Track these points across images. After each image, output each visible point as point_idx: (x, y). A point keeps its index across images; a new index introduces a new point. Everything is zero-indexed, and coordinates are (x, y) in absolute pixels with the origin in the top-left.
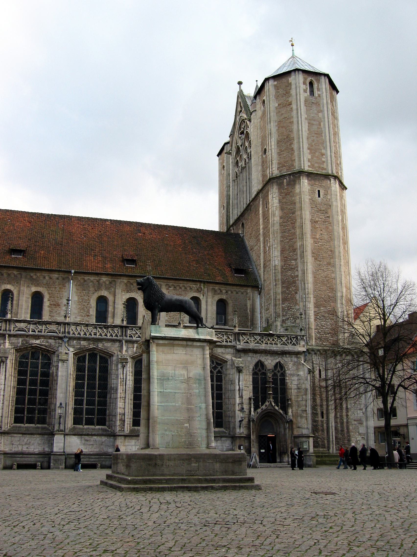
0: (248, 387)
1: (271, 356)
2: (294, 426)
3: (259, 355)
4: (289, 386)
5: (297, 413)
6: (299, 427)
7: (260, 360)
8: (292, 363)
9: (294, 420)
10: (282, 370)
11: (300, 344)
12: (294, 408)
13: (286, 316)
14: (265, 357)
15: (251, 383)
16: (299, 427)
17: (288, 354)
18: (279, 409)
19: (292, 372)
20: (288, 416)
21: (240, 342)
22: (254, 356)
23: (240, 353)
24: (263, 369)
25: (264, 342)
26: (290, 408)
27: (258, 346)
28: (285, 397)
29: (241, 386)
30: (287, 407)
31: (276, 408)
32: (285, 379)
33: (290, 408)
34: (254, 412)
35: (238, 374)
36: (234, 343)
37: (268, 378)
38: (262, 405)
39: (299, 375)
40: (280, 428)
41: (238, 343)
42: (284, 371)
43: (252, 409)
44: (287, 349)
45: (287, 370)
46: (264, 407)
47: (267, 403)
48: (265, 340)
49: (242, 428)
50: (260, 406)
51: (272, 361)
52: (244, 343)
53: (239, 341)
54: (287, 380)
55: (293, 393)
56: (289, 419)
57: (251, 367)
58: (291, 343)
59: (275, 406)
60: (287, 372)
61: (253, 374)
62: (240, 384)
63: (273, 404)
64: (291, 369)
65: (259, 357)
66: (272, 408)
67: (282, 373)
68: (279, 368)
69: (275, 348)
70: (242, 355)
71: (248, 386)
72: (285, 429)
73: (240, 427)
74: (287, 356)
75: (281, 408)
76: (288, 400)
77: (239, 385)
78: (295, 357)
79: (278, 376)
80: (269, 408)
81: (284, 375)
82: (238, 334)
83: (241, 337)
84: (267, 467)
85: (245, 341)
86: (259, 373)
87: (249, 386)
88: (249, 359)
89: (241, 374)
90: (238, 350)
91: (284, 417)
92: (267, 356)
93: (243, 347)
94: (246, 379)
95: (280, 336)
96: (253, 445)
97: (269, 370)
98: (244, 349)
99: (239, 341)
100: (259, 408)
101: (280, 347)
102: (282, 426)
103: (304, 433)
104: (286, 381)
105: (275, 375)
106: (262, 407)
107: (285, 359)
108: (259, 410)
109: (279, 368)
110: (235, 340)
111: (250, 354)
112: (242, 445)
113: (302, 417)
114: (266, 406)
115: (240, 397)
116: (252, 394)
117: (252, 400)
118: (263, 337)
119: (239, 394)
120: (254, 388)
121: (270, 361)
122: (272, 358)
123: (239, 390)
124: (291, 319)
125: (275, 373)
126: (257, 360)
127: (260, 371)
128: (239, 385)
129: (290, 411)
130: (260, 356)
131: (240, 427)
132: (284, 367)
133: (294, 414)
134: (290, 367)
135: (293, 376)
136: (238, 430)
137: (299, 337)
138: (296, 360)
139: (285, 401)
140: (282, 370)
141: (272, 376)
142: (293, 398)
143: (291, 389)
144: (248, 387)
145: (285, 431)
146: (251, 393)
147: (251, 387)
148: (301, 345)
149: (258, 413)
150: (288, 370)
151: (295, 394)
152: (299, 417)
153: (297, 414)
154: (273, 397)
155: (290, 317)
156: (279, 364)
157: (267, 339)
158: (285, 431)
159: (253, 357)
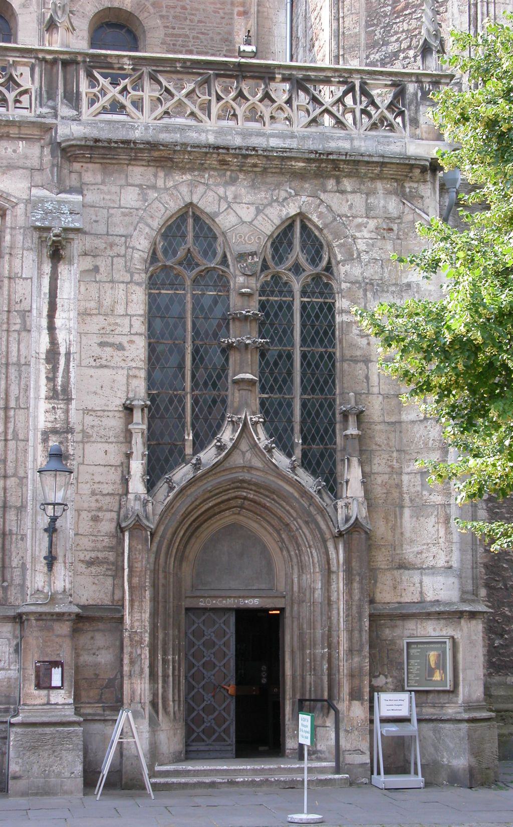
0: (120, 347)
1: (253, 186)
2: (381, 559)
3: (188, 177)
4: (353, 346)
5: (399, 486)
6: (403, 566)
7: (191, 204)
8: (372, 224)
9: (381, 529)
10: (315, 259)
11: (415, 122)
12: (379, 465)
13: (386, 43)
14: (221, 191)
15: (139, 326)
16: (403, 566)
17: (349, 175)
18: (293, 469)
19: (371, 272)
20: (341, 503)
21: (77, 107)
22: (160, 183)
23: (77, 166)
24: (209, 251)
25: (215, 108)
26: (355, 461)
27: (182, 129)
28: (331, 406)
29: (61, 336)
30: (338, 456)
31: (280, 459)
32: (331, 308)
33: (355, 461)
34: (150, 485)
35: (47, 268)
36: (45, 110)
37: (235, 301)
38: (199, 445)
39: (409, 285)
40: (302, 568)
41: (65, 111)
42: (328, 268)
43: (137, 466)
44: (346, 145)
45: (344, 262)
46: (209, 456)
47: (227, 435)
48: (219, 98)
49: (59, 567)
50: (189, 450)
51: (258, 211)
52: (105, 110)
53: (73, 99)
54: (342, 311)
55: (374, 379)
56: (347, 519)
57: (142, 244)
58: (364, 112)
59: (270, 450)
60: (343, 269)
61: (153, 283)
62: (58, 322)
63: (262, 439)
64: (365, 257)
65: (184, 190)
66: (257, 463)
67: (317, 278)
68: (297, 253)
69: (274, 142)
70: (91, 174)
71: (117, 340)
72: (328, 572)
73: (51, 560)
74: (348, 184)
75: (309, 463)
76: (345, 415)
77: (51, 328)
78: (388, 193)
79: (291, 293)
80: (237, 459)
81: (327, 285)
82: (65, 64)
83: (84, 86)
84: (213, 785)
85: (104, 101)
86: (189, 276)
87: (124, 340)
88: (130, 197)
89: (63, 268)
90: (64, 150)
91: (322, 511)
92: (233, 181)
93: (95, 133)
94: (107, 302)
95: (308, 79)
96: (132, 662)
97: (242, 257)
98: (97, 141)
99: (73, 99)
100: (182, 459)
101: (304, 138)
102: (314, 557)
103: (430, 596)
104: (338, 319)
105: (276, 285)
106: (201, 455)
107: (334, 200)
108: (182, 474)
109: (297, 253)
110: (51, 96)
111: (139, 173)
112: (56, 664)
113: (420, 509)
114: (220, 448)
115: (53, 395)
116: (140, 387)
117: (137, 416)
118: (207, 81)
119: (51, 379)
120: (154, 357)
121: (247, 213)
122: (262, 196)
123: (52, 355)
124: (405, 58)
125: (276, 277)
126: (173, 206)
127: (189, 261)
128: (51, 328)
129: (353, 475)
130: (192, 185)
131: (51, 560)
132: (329, 246)
133: (379, 491)
134: (361, 245)
135: (375, 294)
136: (38, 580)
137: (411, 88)
138: (393, 205)
139: (332, 423)
140: (315, 259)
141: (262, 292)
142: (375, 408)
143: (367, 361)
144: (120, 347)
145: (327, 583)
146: (135, 383)
147: (138, 349)
148: (423, 126)
149: (171, 488)
150: (351, 257)
151: (385, 389)
152: (407, 512)
153: (396, 494)
154: (262, 403)
155: (404, 45)
156: (304, 227)
157: (233, 94)
158: (327, 583)
159: (154, 187)
